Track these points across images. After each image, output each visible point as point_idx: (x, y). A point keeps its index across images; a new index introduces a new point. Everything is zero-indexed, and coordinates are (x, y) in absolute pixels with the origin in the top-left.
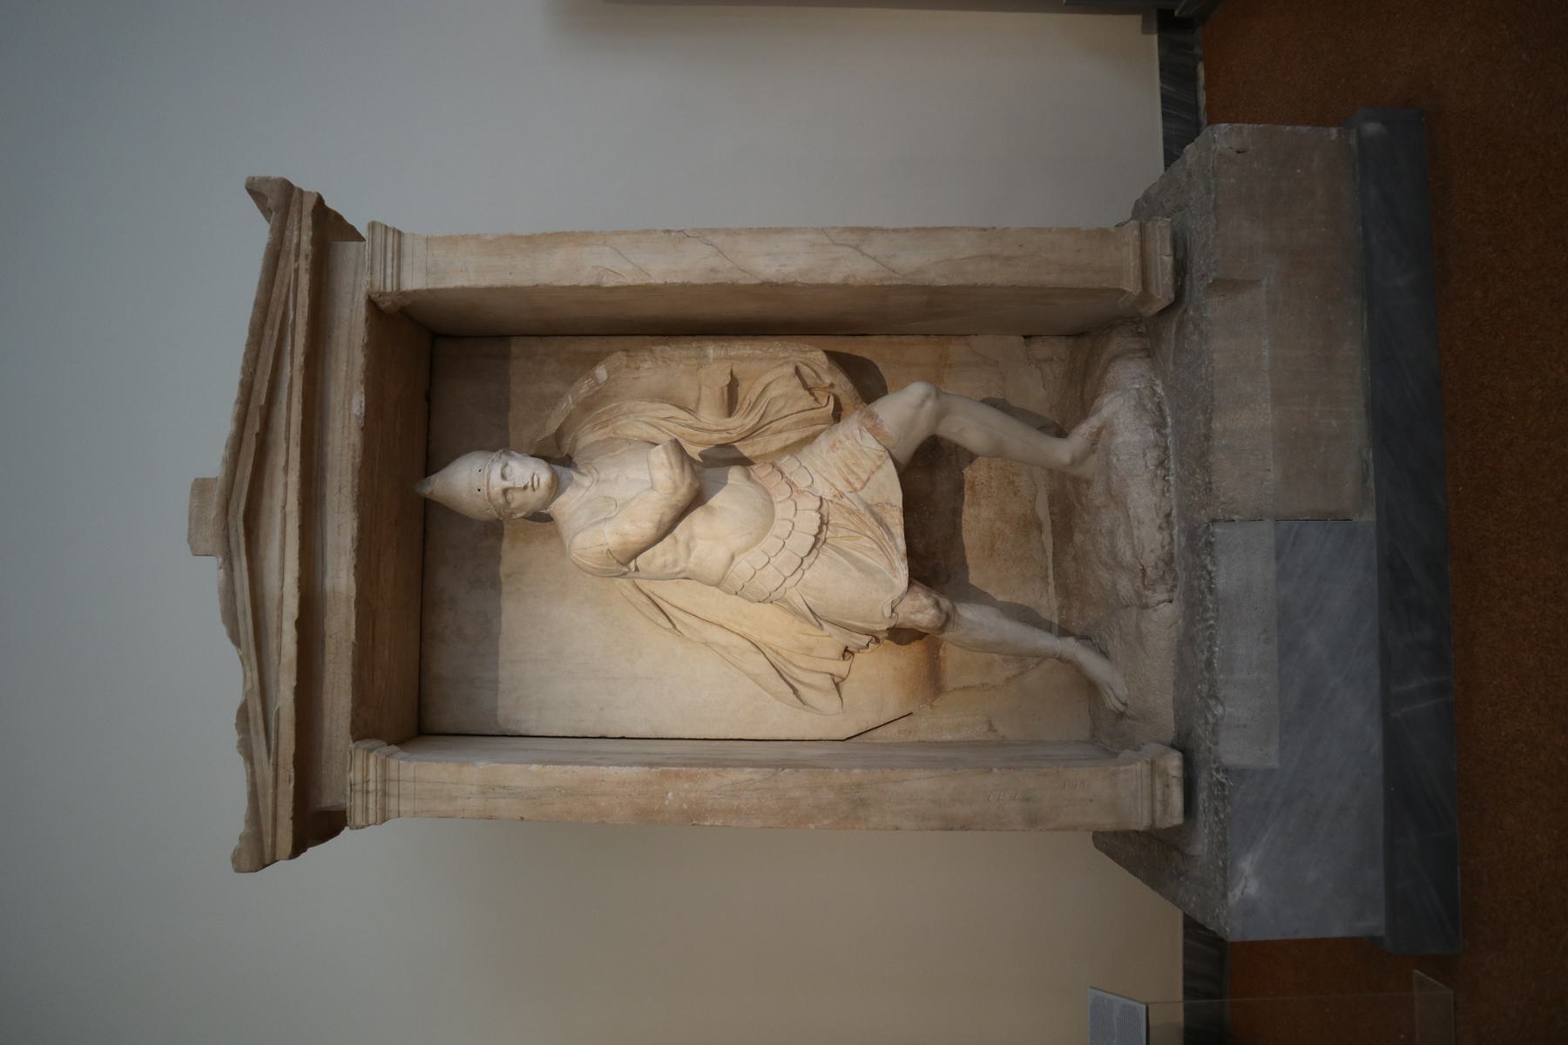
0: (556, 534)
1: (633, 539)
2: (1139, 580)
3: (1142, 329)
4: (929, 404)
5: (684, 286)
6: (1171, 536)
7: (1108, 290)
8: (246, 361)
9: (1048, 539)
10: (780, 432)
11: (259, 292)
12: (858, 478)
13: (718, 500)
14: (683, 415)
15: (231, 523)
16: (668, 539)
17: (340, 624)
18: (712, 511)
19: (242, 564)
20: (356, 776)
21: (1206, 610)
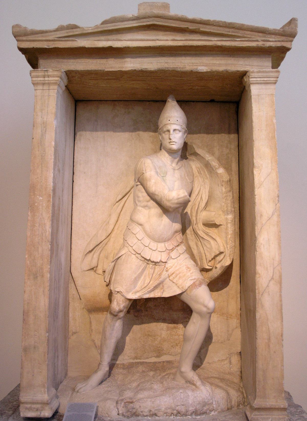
1: (148, 183)
2: (129, 400)
3: (241, 407)
4: (205, 309)
5: (254, 203)
8: (218, 22)
9: (153, 360)
10: (197, 246)
13: (166, 220)
14: (203, 205)
15: (151, 19)
16: (148, 198)
18: (160, 216)
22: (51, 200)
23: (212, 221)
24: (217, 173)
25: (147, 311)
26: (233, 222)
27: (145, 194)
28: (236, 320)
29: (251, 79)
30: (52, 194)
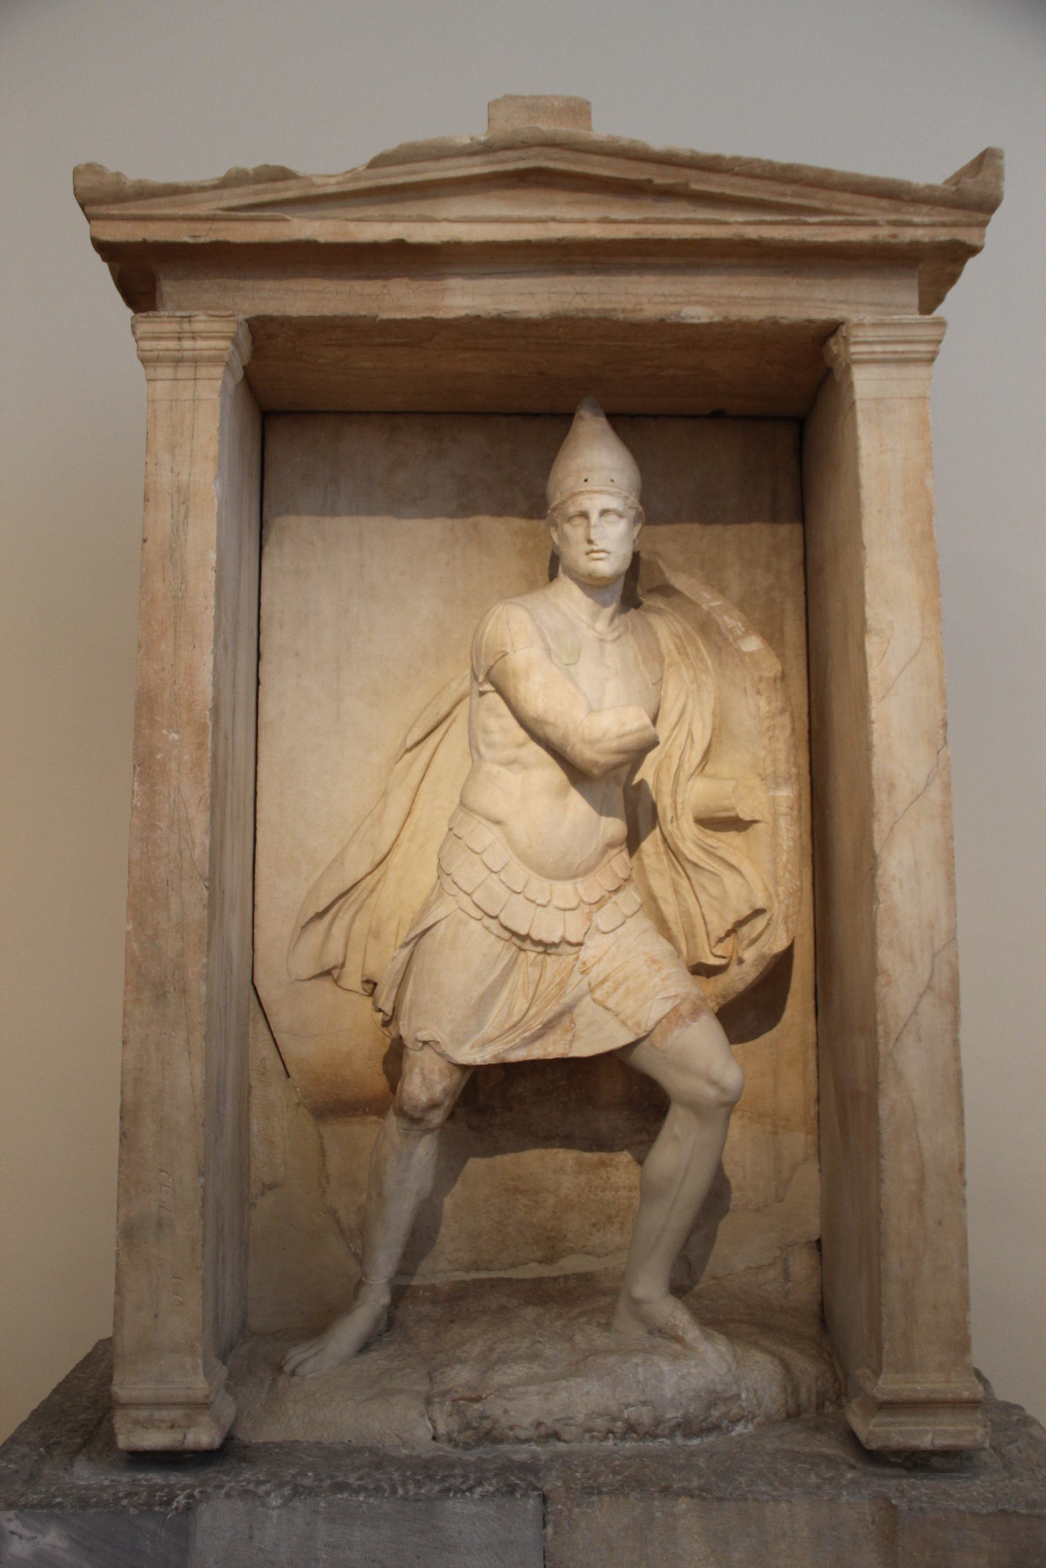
0: (532, 586)
3: (829, 1409)
4: (711, 1092)
5: (869, 748)
6: (527, 1440)
7: (880, 1349)
8: (749, 162)
9: (533, 1271)
10: (676, 892)
11: (842, 175)
12: (608, 995)
13: (577, 803)
14: (695, 756)
15: (532, 151)
16: (522, 734)
17: (402, 299)
18: (562, 794)
19: (478, 167)
20: (202, 324)
21: (419, 1484)
22: (209, 741)
23: (726, 810)
24: (738, 651)
25: (510, 1110)
26: (795, 812)
27: (511, 722)
29: (853, 349)
30: (210, 723)
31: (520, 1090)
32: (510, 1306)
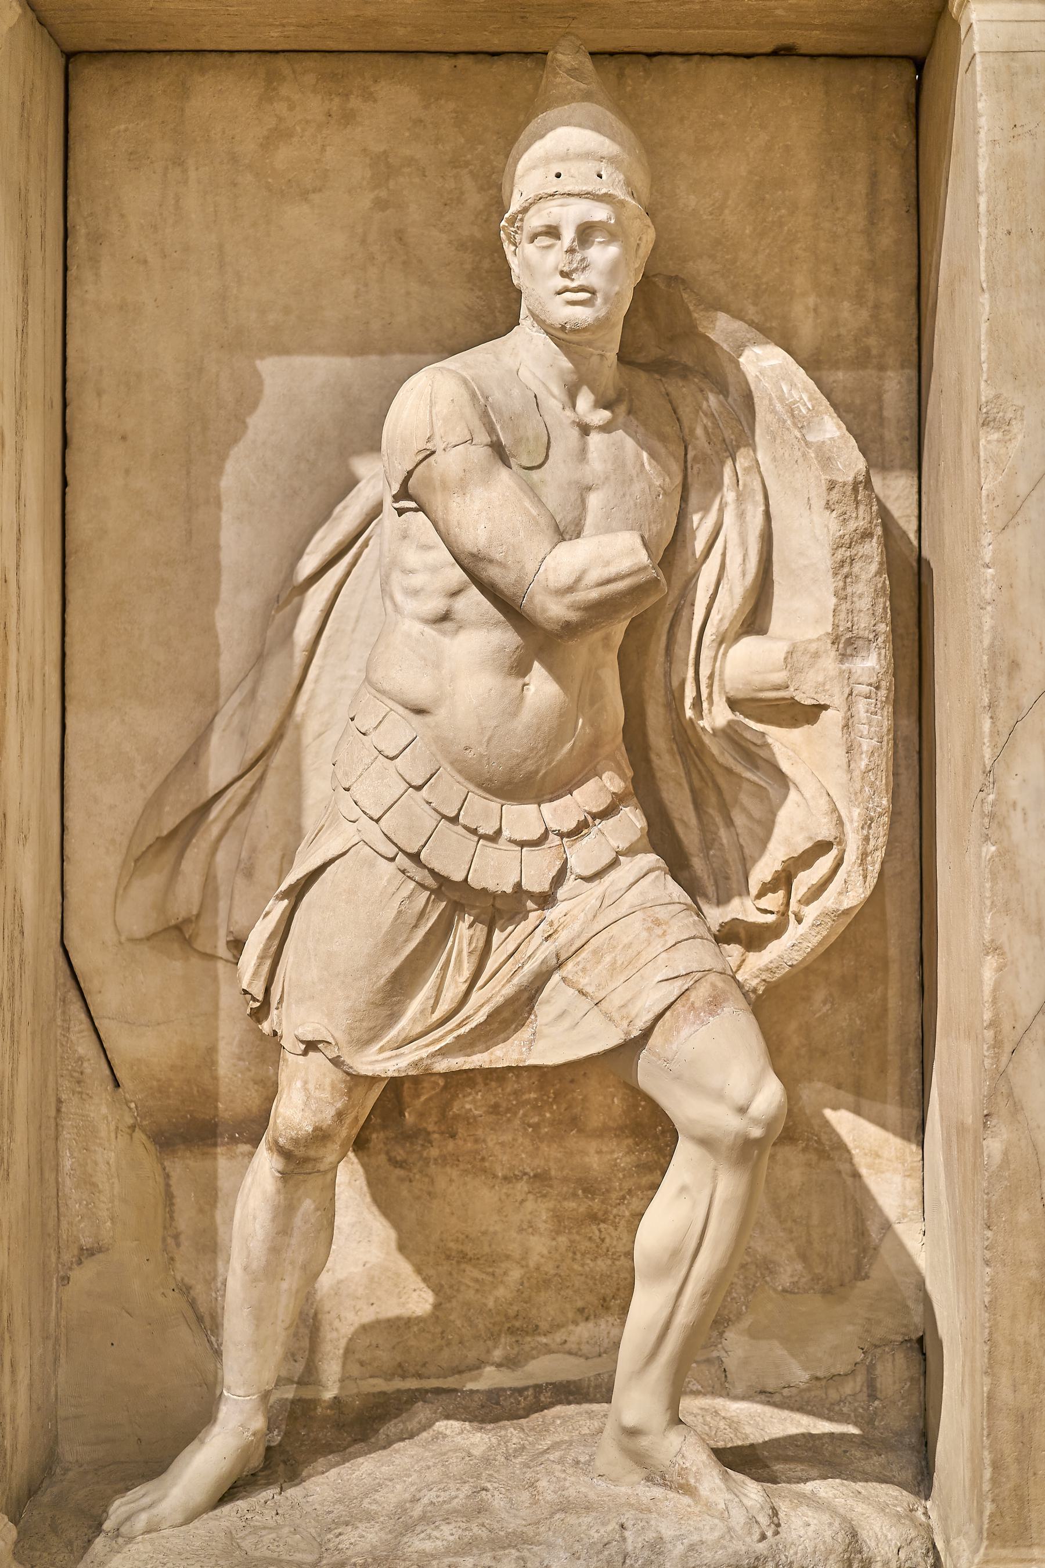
25: (453, 1136)
28: (898, 1179)
31: (468, 1106)
32: (448, 1432)
